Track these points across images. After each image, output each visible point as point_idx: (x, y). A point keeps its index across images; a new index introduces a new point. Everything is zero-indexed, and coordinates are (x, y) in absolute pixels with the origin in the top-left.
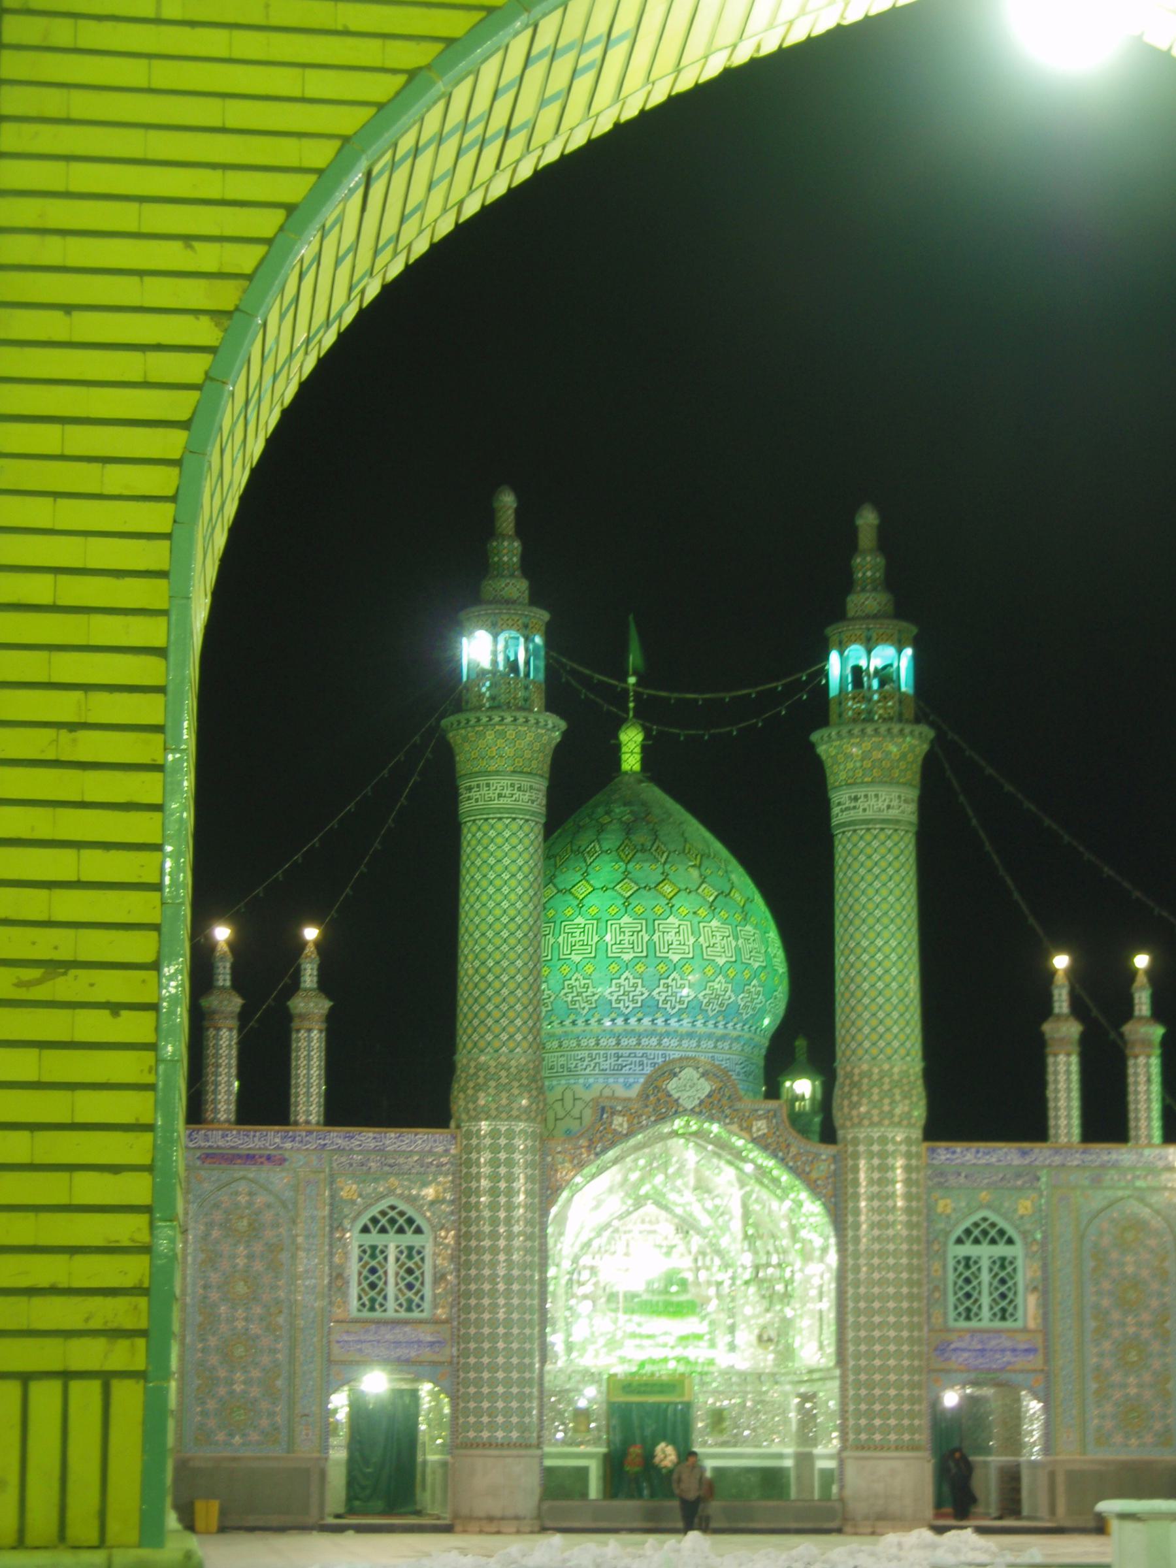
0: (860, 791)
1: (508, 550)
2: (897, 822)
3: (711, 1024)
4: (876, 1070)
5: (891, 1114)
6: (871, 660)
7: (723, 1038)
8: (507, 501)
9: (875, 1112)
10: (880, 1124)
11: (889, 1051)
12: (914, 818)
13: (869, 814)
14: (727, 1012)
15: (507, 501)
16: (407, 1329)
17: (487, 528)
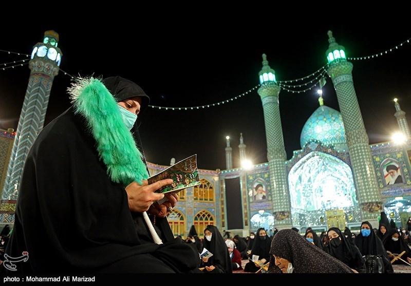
0: (337, 78)
1: (265, 62)
2: (346, 82)
3: (338, 141)
4: (352, 132)
5: (357, 141)
6: (336, 55)
7: (342, 143)
8: (264, 56)
9: (353, 141)
10: (355, 143)
11: (354, 127)
12: (352, 80)
13: (340, 82)
14: (341, 138)
15: (264, 56)
16: (263, 203)
17: (262, 60)
